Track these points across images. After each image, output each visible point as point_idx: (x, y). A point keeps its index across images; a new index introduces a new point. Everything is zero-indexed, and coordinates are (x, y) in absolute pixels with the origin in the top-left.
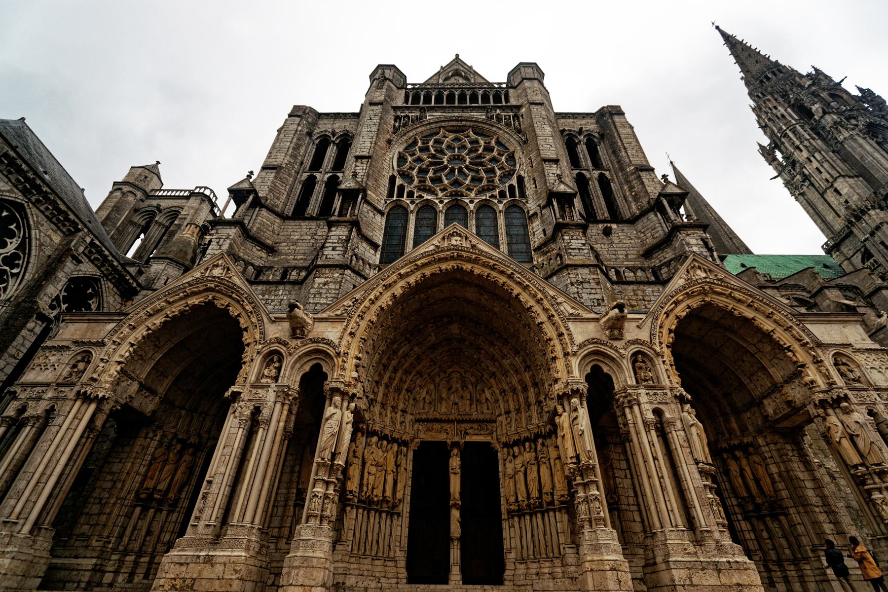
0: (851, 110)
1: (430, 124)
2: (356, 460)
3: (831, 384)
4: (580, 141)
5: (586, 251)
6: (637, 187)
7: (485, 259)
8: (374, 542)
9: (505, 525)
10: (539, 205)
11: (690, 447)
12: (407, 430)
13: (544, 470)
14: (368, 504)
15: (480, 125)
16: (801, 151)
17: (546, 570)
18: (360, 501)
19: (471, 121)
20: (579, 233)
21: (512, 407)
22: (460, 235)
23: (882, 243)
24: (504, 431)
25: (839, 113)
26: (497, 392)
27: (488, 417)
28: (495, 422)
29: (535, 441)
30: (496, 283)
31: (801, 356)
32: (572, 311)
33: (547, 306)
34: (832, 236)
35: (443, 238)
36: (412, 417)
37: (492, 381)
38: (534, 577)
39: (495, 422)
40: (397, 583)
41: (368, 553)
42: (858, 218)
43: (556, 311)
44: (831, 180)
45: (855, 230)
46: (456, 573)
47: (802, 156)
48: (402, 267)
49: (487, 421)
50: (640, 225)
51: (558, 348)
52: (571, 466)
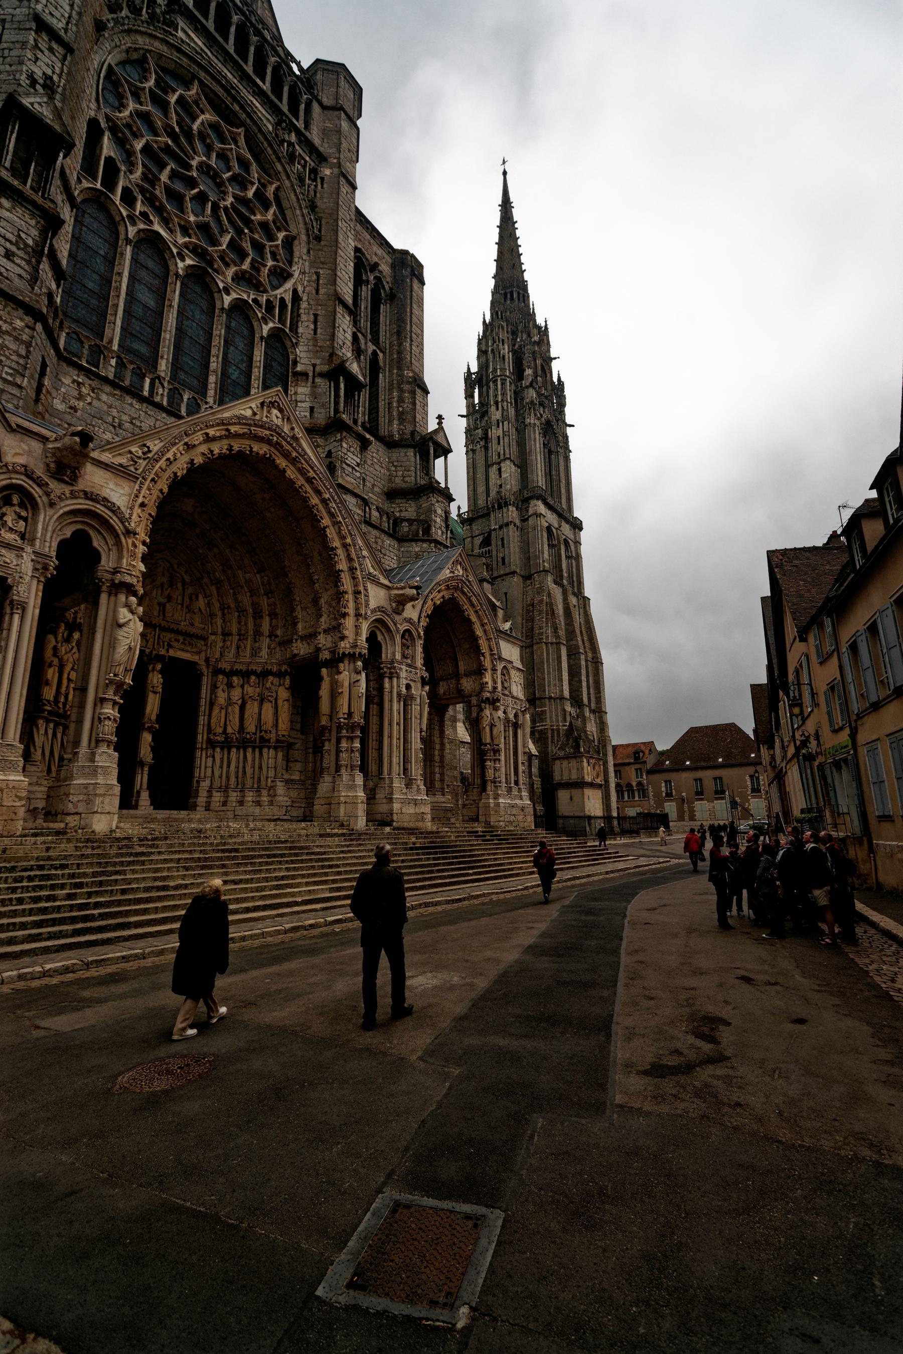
0: (546, 397)
1: (179, 50)
3: (495, 688)
4: (368, 282)
5: (358, 474)
6: (407, 405)
7: (306, 466)
10: (314, 366)
11: (420, 719)
15: (259, 135)
16: (497, 409)
17: (250, 799)
19: (249, 115)
20: (356, 445)
21: (234, 630)
22: (281, 410)
23: (503, 539)
25: (539, 394)
26: (217, 605)
27: (199, 632)
28: (205, 639)
30: (306, 500)
31: (487, 663)
32: (372, 570)
33: (354, 556)
34: (472, 508)
35: (262, 404)
37: (213, 588)
42: (500, 507)
43: (360, 565)
44: (502, 457)
45: (492, 515)
46: (145, 797)
47: (496, 415)
48: (213, 426)
50: (397, 454)
51: (351, 605)
52: (342, 720)
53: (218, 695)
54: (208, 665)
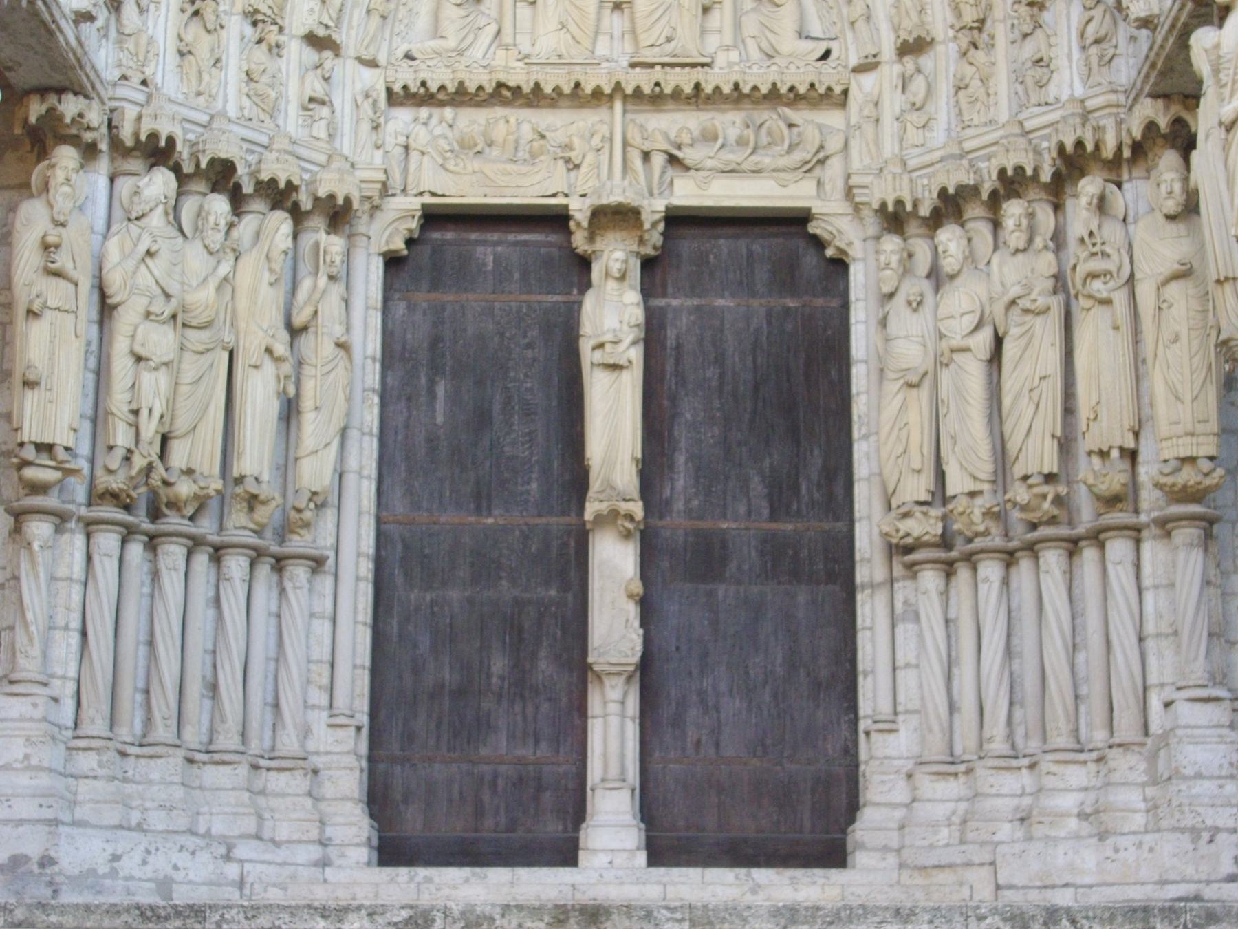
2: (56, 292)
8: (195, 689)
9: (870, 611)
12: (345, 144)
13: (1098, 339)
14: (144, 509)
18: (98, 496)
24: (889, 148)
27: (799, 76)
29: (1058, 191)
36: (367, 74)
38: (1005, 831)
39: (842, 99)
40: (324, 863)
41: (163, 732)
49: (795, 98)
53: (893, 327)
54: (857, 208)
